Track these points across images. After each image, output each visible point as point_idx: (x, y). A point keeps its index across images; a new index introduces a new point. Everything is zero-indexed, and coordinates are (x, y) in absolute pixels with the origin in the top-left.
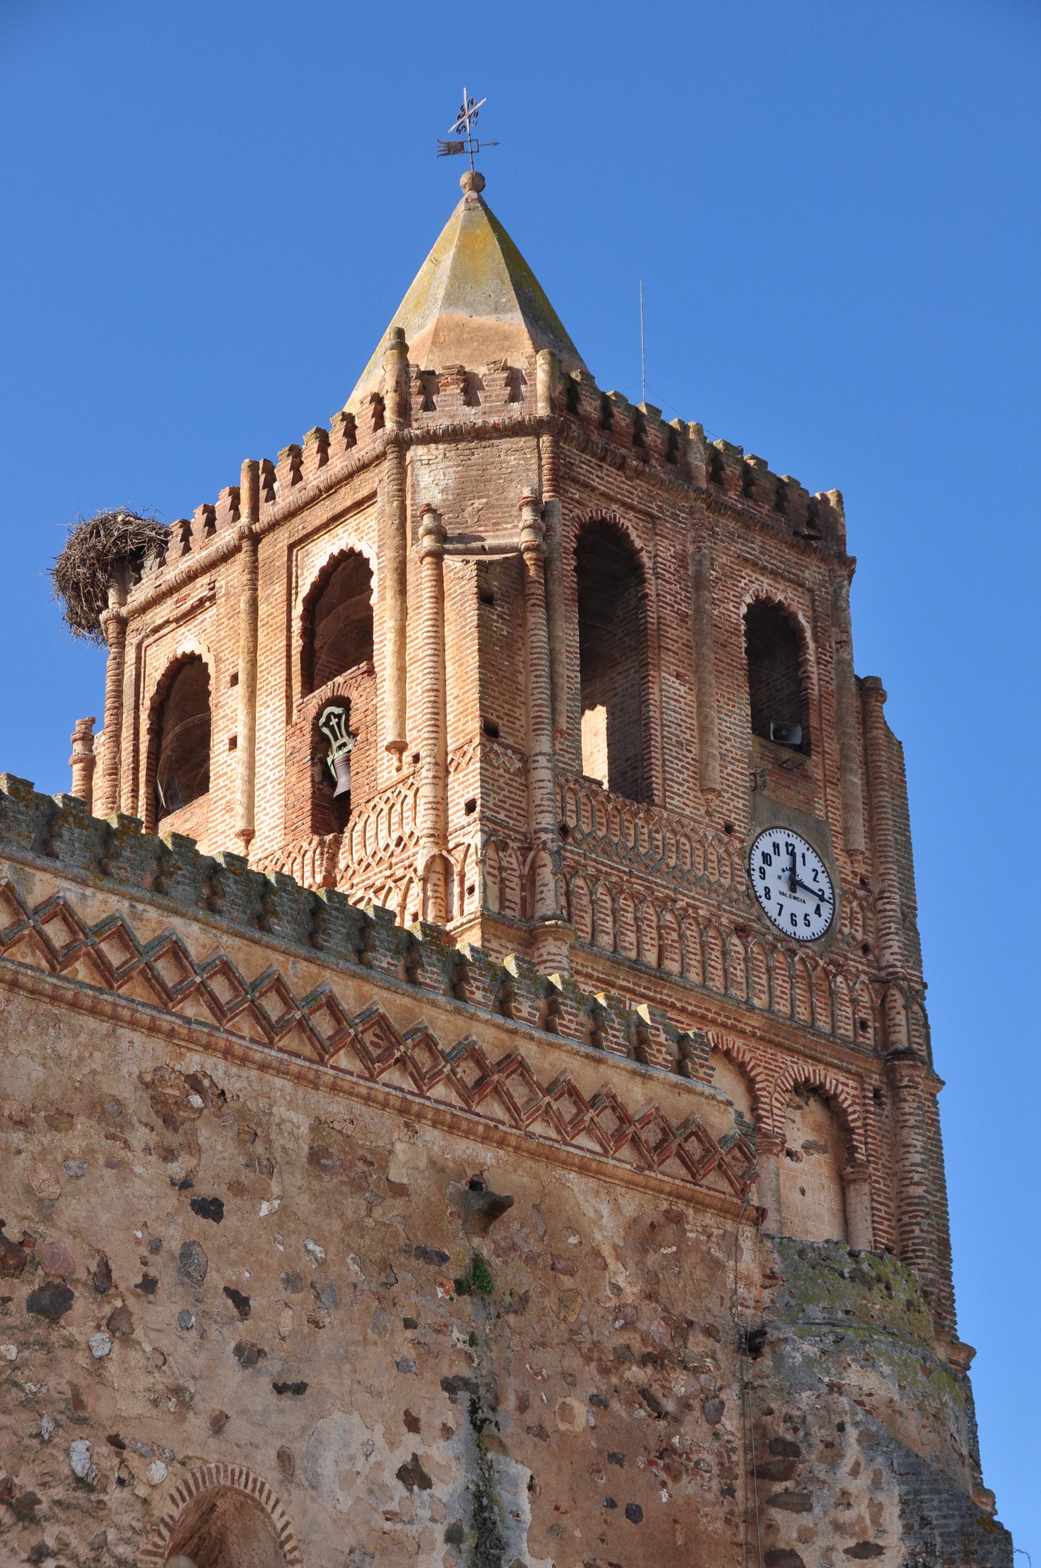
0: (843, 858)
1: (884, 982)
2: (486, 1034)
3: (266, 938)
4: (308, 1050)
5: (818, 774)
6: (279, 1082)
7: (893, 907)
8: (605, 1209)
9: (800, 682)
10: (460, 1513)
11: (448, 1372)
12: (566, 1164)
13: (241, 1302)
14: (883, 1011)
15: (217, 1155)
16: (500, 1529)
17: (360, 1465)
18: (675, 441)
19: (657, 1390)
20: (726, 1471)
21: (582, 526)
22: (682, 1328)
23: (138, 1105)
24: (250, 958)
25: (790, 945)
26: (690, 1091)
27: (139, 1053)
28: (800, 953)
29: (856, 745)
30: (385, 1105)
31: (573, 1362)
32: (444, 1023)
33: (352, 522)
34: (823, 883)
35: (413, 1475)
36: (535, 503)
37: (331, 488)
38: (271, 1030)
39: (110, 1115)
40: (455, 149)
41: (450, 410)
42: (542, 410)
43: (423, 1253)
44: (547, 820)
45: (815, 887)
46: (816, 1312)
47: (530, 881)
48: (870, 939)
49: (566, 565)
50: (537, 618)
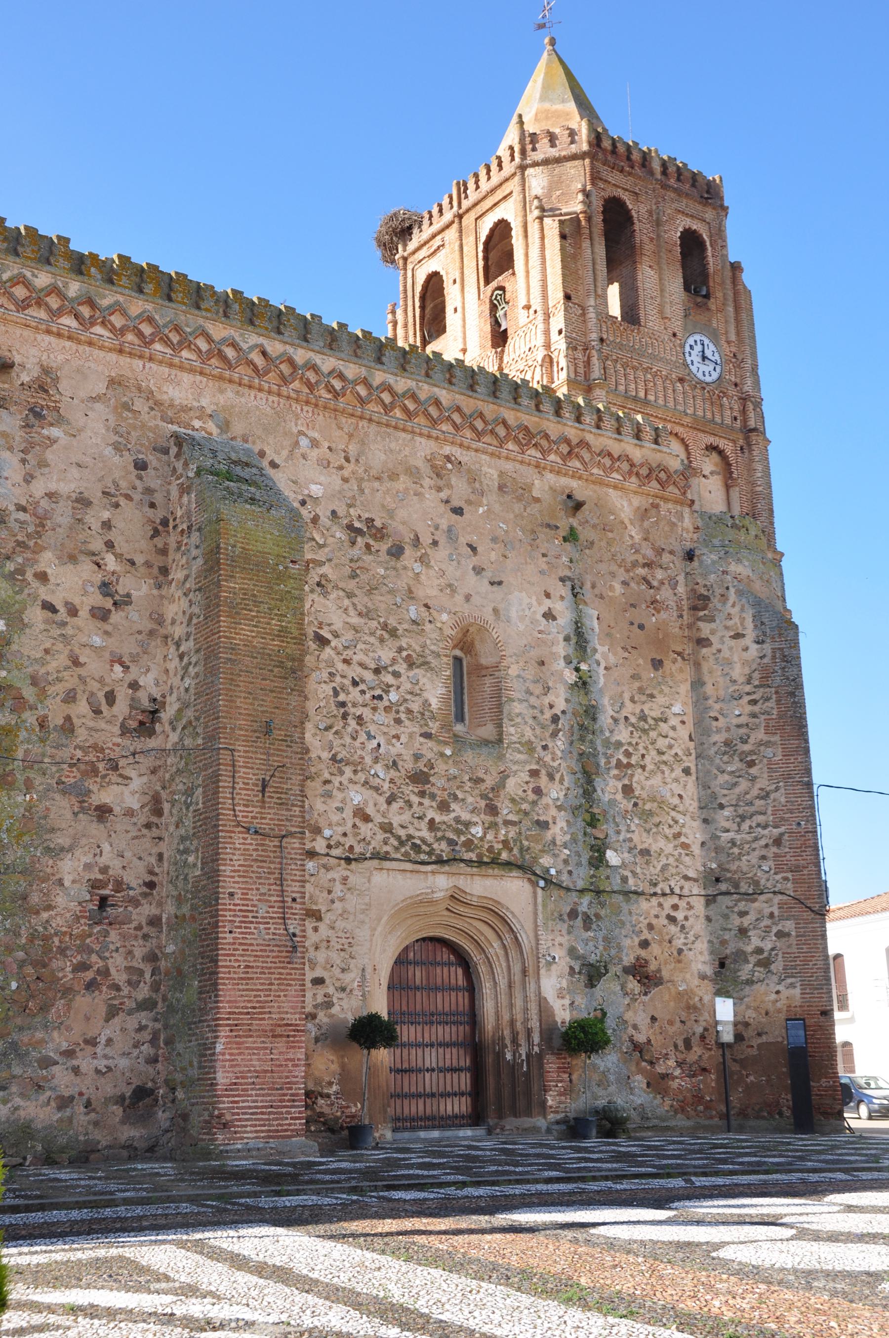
0: (725, 345)
1: (744, 399)
2: (572, 432)
3: (475, 395)
4: (495, 443)
5: (713, 307)
6: (484, 457)
7: (748, 366)
8: (625, 504)
9: (704, 267)
10: (570, 630)
11: (562, 574)
12: (608, 486)
13: (474, 549)
14: (744, 412)
16: (586, 636)
17: (527, 612)
18: (645, 157)
19: (650, 578)
20: (679, 608)
21: (605, 200)
22: (660, 551)
23: (425, 469)
24: (469, 404)
25: (703, 386)
26: (660, 451)
27: (424, 447)
28: (707, 389)
29: (730, 294)
30: (529, 464)
31: (614, 568)
32: (553, 428)
33: (502, 206)
34: (717, 357)
35: (549, 615)
36: (583, 191)
37: (493, 191)
38: (479, 434)
39: (413, 473)
40: (542, 26)
41: (544, 150)
42: (585, 147)
43: (548, 526)
44: (594, 336)
45: (713, 359)
46: (716, 542)
47: (588, 363)
48: (738, 381)
49: (598, 219)
50: (586, 244)
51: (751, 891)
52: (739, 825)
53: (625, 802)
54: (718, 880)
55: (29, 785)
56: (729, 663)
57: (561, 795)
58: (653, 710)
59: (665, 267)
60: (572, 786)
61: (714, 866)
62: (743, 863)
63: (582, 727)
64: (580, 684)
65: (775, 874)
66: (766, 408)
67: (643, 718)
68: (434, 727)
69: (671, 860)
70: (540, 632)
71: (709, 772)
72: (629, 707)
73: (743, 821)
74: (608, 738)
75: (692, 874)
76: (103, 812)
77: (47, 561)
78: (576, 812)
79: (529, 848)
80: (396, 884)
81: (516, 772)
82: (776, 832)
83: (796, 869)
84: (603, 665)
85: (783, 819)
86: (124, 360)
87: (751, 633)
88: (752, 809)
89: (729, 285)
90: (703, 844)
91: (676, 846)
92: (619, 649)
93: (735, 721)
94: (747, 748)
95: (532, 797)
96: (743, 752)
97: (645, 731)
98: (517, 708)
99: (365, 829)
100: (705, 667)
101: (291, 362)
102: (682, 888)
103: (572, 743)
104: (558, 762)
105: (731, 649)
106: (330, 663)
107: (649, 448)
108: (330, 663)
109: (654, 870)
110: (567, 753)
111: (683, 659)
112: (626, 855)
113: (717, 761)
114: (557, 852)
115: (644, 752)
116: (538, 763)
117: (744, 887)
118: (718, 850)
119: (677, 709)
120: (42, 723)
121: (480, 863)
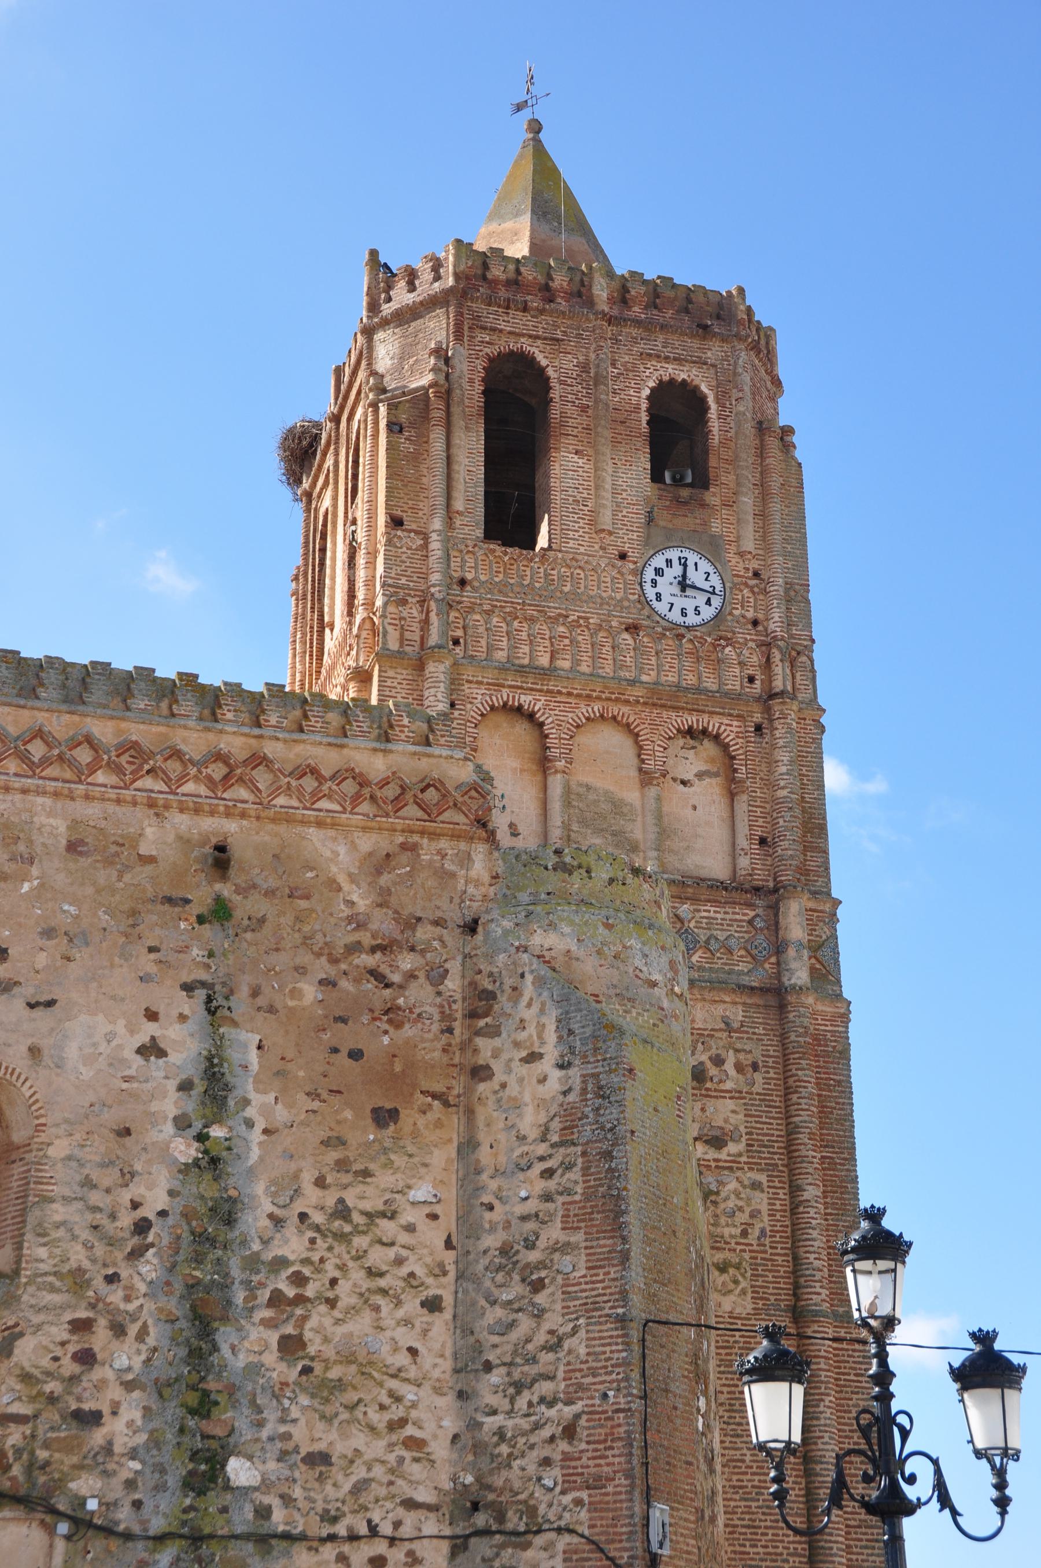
0: (735, 560)
2: (234, 741)
3: (38, 704)
4: (68, 775)
6: (40, 800)
8: (342, 850)
10: (194, 1071)
11: (186, 977)
12: (304, 822)
16: (228, 1077)
17: (103, 1047)
19: (384, 969)
21: (491, 360)
25: (679, 632)
26: (429, 756)
28: (688, 636)
30: (135, 804)
31: (304, 958)
32: (193, 740)
34: (715, 580)
35: (152, 1050)
41: (402, 297)
43: (169, 900)
45: (706, 586)
47: (426, 622)
48: (760, 616)
49: (471, 392)
51: (522, 1529)
52: (512, 1402)
53: (282, 1367)
54: (475, 1507)
56: (517, 1105)
57: (137, 1362)
58: (362, 1198)
59: (607, 450)
60: (166, 1343)
61: (469, 1479)
62: (514, 1474)
63: (200, 1237)
64: (203, 1163)
65: (563, 1492)
66: (824, 657)
67: (342, 1212)
69: (378, 1471)
70: (127, 1079)
71: (474, 1303)
73: (518, 1393)
74: (257, 1254)
75: (423, 1495)
78: (167, 1392)
79: (48, 1463)
81: (38, 1327)
82: (569, 1411)
83: (595, 1483)
84: (260, 1125)
85: (580, 1387)
87: (551, 1051)
88: (533, 1370)
89: (748, 458)
90: (455, 1437)
91: (391, 1446)
92: (301, 1097)
93: (520, 1209)
94: (533, 1256)
95: (69, 1367)
96: (527, 1265)
97: (342, 1237)
98: (58, 1212)
100: (482, 1114)
102: (397, 1524)
103: (172, 1268)
104: (136, 1303)
105: (521, 1080)
107: (404, 753)
109: (338, 1488)
110: (159, 1288)
111: (446, 1104)
112: (272, 1465)
113: (488, 1283)
114: (111, 1466)
115: (337, 1274)
116: (93, 1306)
117: (514, 1521)
118: (478, 1448)
119: (422, 1192)
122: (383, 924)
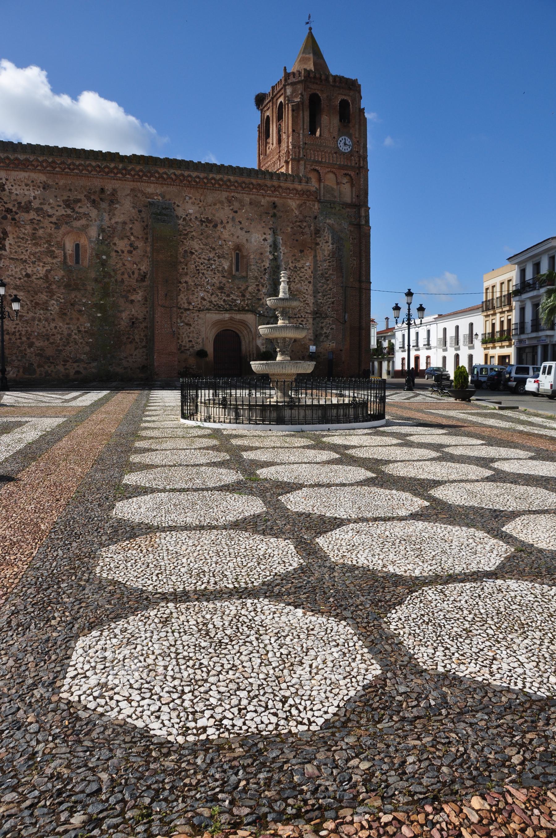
1: (359, 157)
2: (276, 183)
7: (362, 145)
13: (240, 222)
15: (236, 205)
22: (306, 217)
24: (240, 180)
25: (344, 154)
27: (225, 194)
32: (269, 183)
35: (265, 240)
36: (301, 94)
39: (221, 203)
41: (292, 80)
49: (307, 102)
50: (301, 112)
55: (113, 296)
58: (299, 265)
67: (295, 267)
68: (226, 274)
72: (291, 264)
76: (132, 301)
77: (116, 240)
80: (213, 317)
83: (337, 311)
86: (135, 183)
87: (330, 241)
98: (253, 267)
99: (204, 303)
101: (183, 175)
106: (194, 259)
108: (194, 259)
120: (116, 281)
121: (239, 310)
122: (301, 217)
